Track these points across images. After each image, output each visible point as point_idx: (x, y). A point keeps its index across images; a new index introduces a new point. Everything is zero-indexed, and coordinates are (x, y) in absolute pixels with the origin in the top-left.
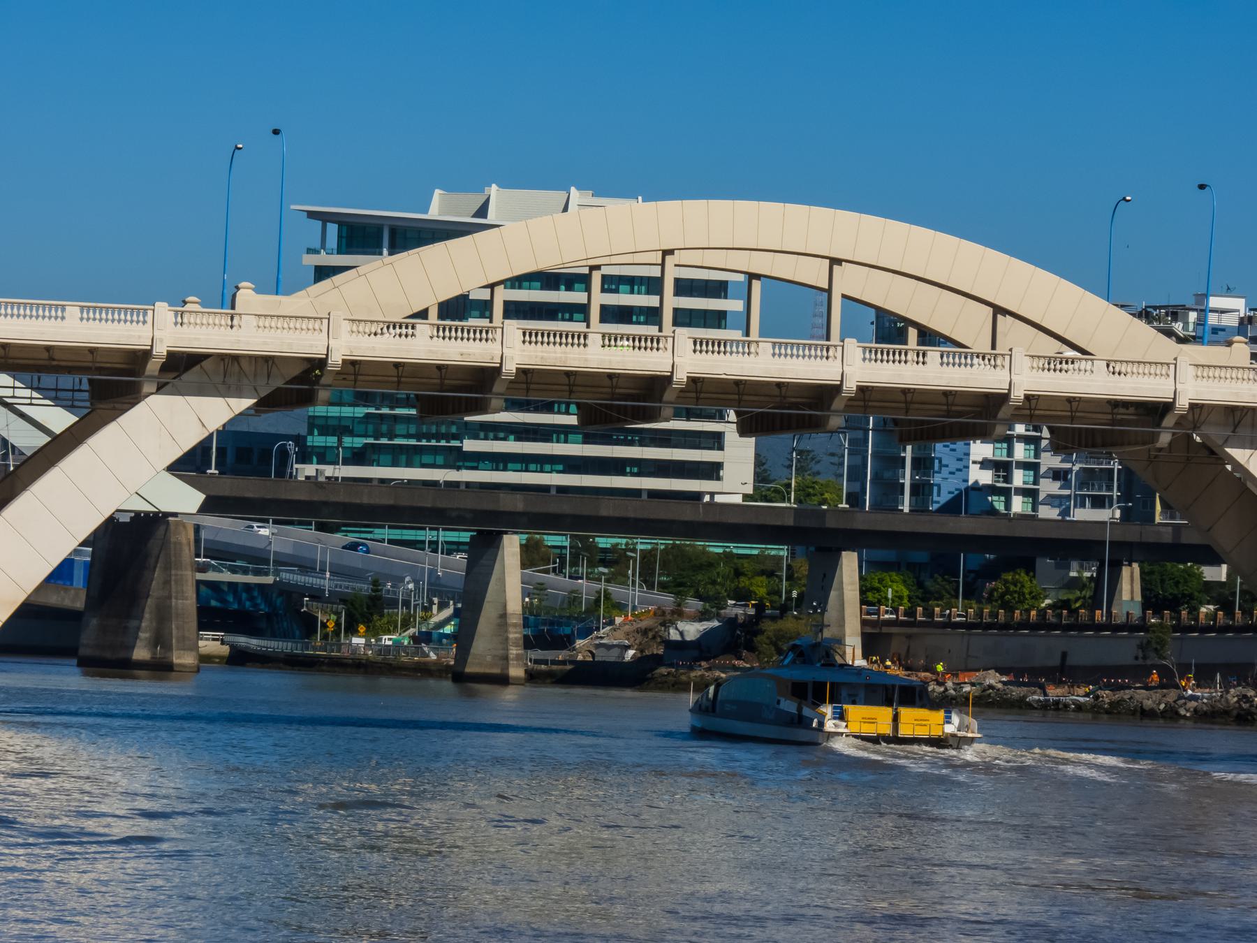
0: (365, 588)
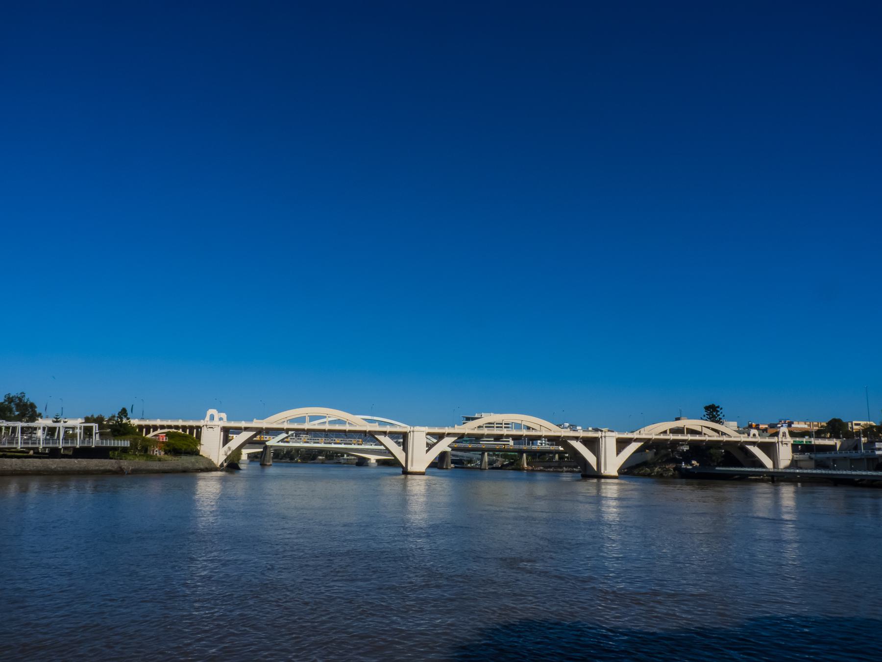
0: (470, 459)
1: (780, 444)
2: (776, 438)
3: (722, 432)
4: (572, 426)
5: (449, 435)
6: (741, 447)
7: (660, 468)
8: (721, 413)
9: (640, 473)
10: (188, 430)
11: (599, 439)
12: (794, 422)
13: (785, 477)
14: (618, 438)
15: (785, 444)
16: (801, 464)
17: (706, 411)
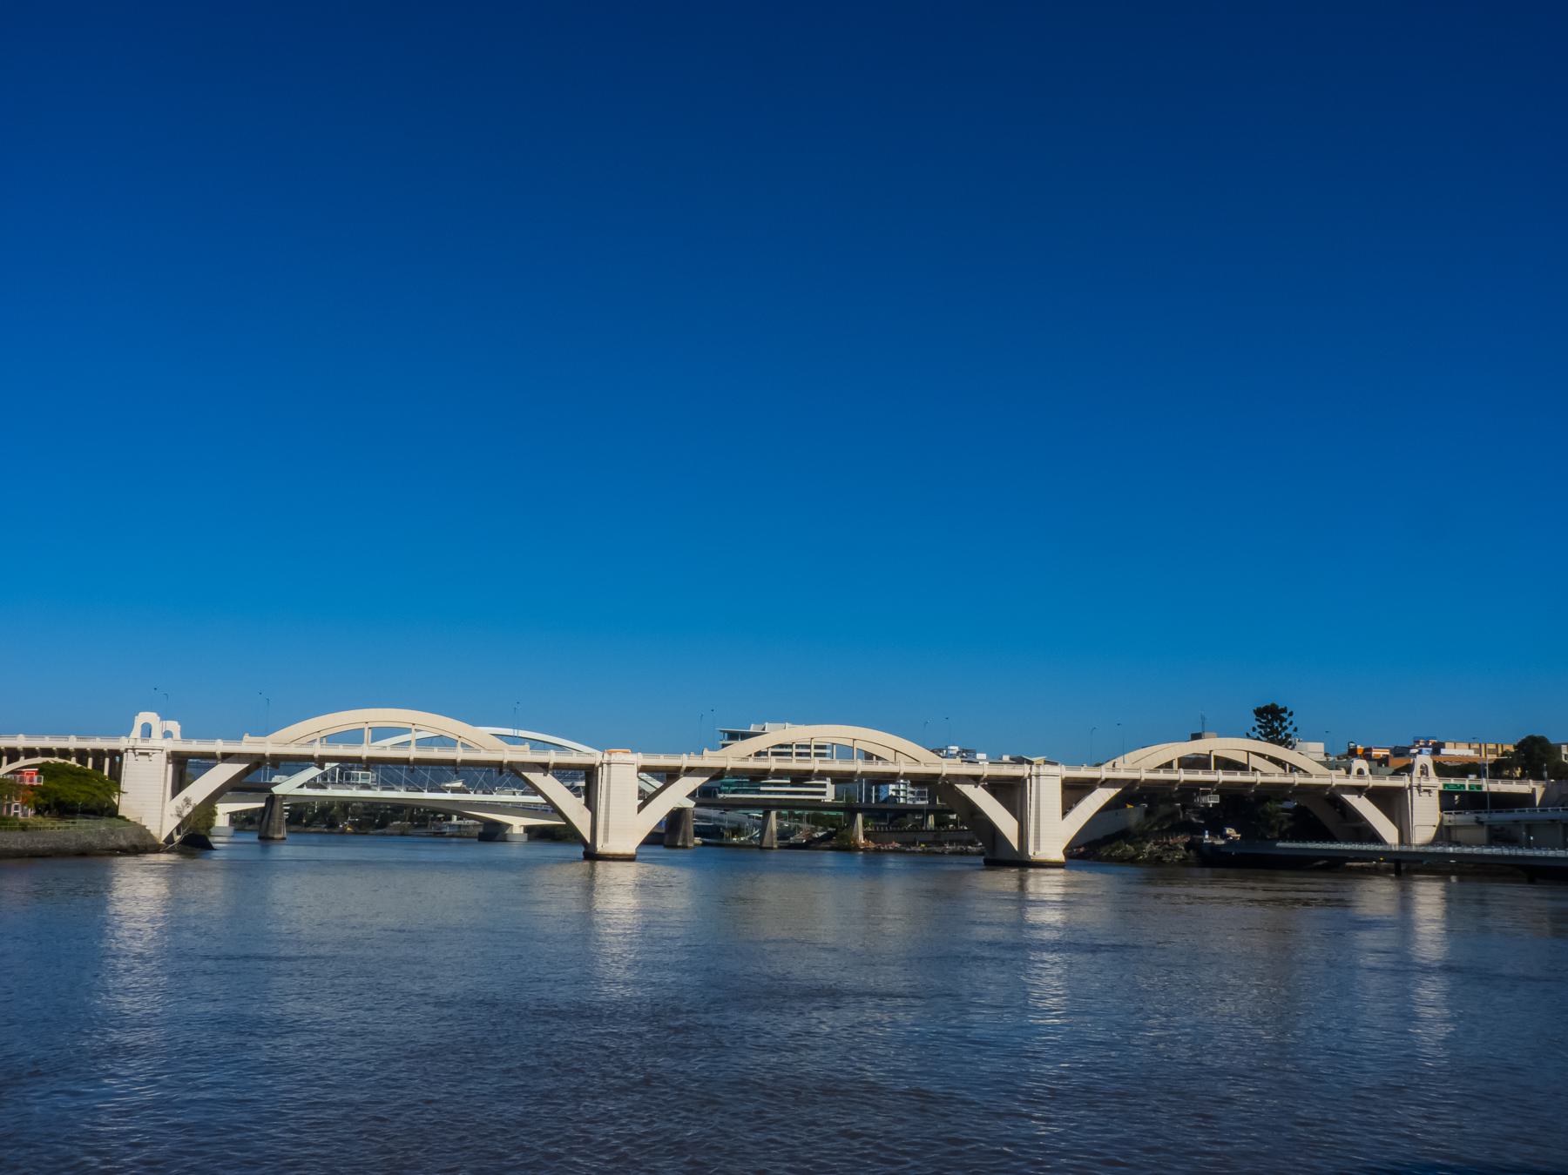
0: (735, 825)
1: (1415, 791)
2: (1407, 778)
3: (1290, 764)
4: (964, 751)
5: (690, 771)
6: (1331, 798)
7: (1155, 844)
8: (1291, 723)
9: (1113, 855)
10: (90, 760)
11: (1026, 780)
12: (1447, 744)
13: (1425, 863)
14: (1066, 778)
15: (1425, 791)
16: (1459, 835)
17: (1257, 720)
